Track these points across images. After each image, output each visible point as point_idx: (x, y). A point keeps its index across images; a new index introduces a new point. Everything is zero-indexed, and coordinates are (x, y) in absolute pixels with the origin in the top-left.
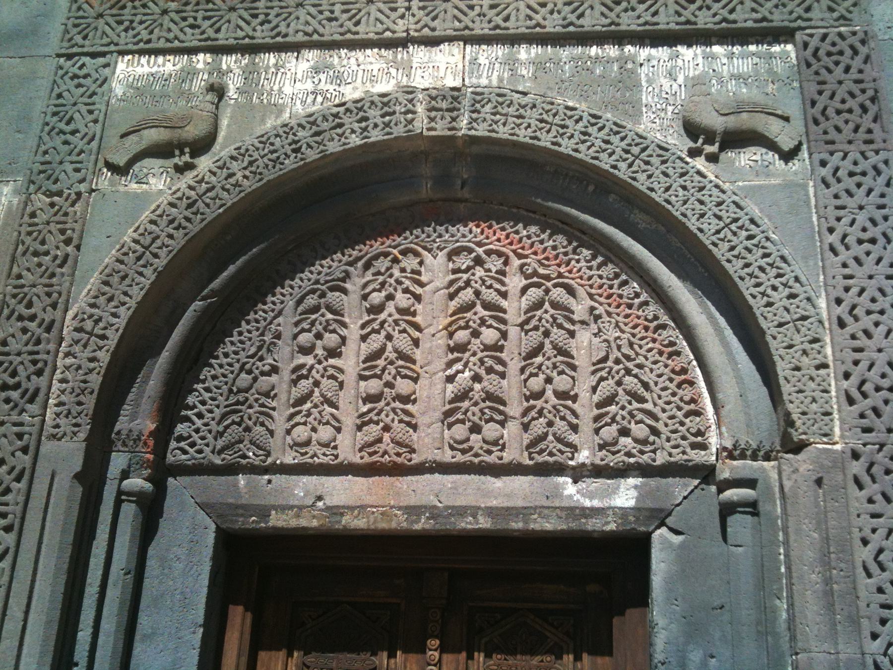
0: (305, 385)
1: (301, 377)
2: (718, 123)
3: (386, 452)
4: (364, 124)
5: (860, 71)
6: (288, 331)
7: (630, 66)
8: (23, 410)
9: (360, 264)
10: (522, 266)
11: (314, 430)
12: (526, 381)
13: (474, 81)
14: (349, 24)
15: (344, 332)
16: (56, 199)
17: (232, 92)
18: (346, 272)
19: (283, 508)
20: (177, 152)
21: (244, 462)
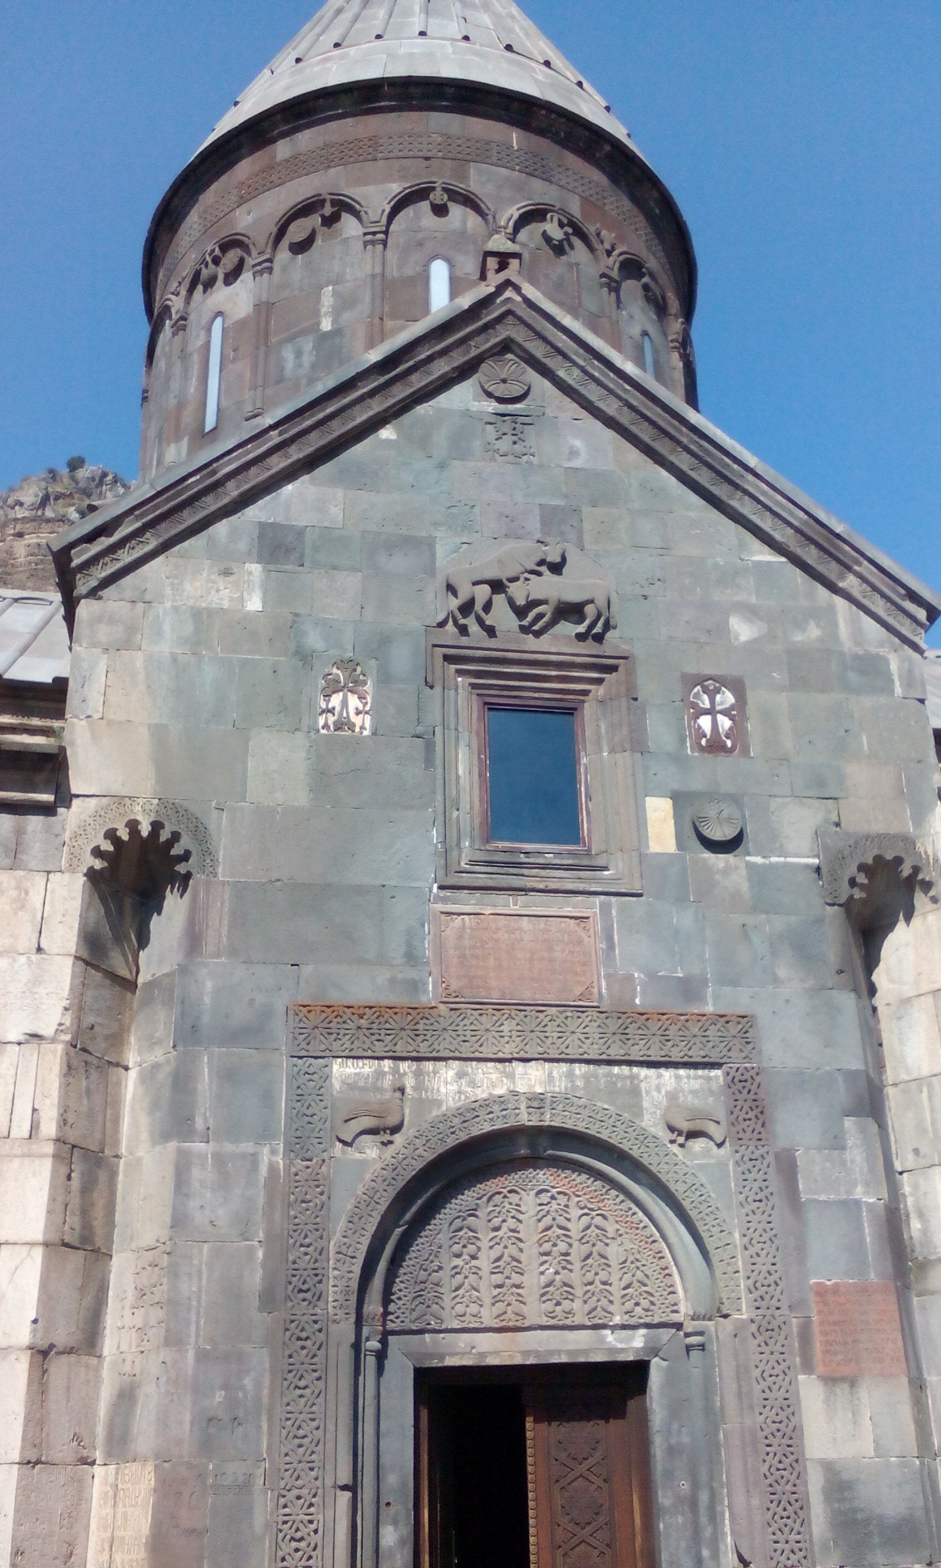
0: (459, 1278)
1: (457, 1273)
2: (685, 1126)
3: (510, 1320)
4: (491, 1116)
5: (756, 1094)
6: (446, 1244)
7: (636, 1082)
8: (315, 1306)
9: (485, 1199)
10: (579, 1202)
11: (467, 1306)
12: (584, 1275)
13: (552, 1089)
14: (476, 1046)
15: (479, 1243)
16: (309, 1163)
17: (408, 1090)
18: (477, 1204)
19: (453, 1354)
20: (382, 1133)
21: (429, 1327)
